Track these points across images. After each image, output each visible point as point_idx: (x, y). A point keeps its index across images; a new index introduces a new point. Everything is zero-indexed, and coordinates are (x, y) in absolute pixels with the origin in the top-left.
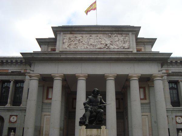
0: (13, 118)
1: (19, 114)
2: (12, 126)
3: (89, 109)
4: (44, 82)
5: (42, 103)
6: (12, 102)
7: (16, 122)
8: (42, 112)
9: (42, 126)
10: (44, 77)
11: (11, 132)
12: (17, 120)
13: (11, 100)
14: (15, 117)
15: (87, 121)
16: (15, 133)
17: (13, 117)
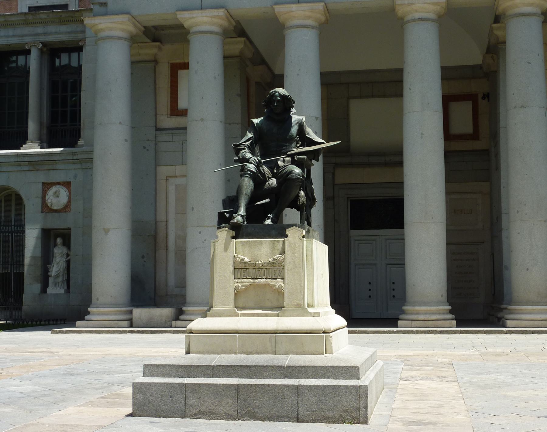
0: (56, 194)
1: (75, 176)
2: (55, 223)
3: (251, 167)
4: (158, 44)
5: (157, 129)
6: (45, 131)
7: (67, 207)
8: (156, 166)
9: (161, 217)
10: (155, 27)
11: (55, 245)
12: (69, 201)
13: (41, 124)
14: (63, 192)
15: (242, 211)
16: (69, 248)
17: (54, 189)
